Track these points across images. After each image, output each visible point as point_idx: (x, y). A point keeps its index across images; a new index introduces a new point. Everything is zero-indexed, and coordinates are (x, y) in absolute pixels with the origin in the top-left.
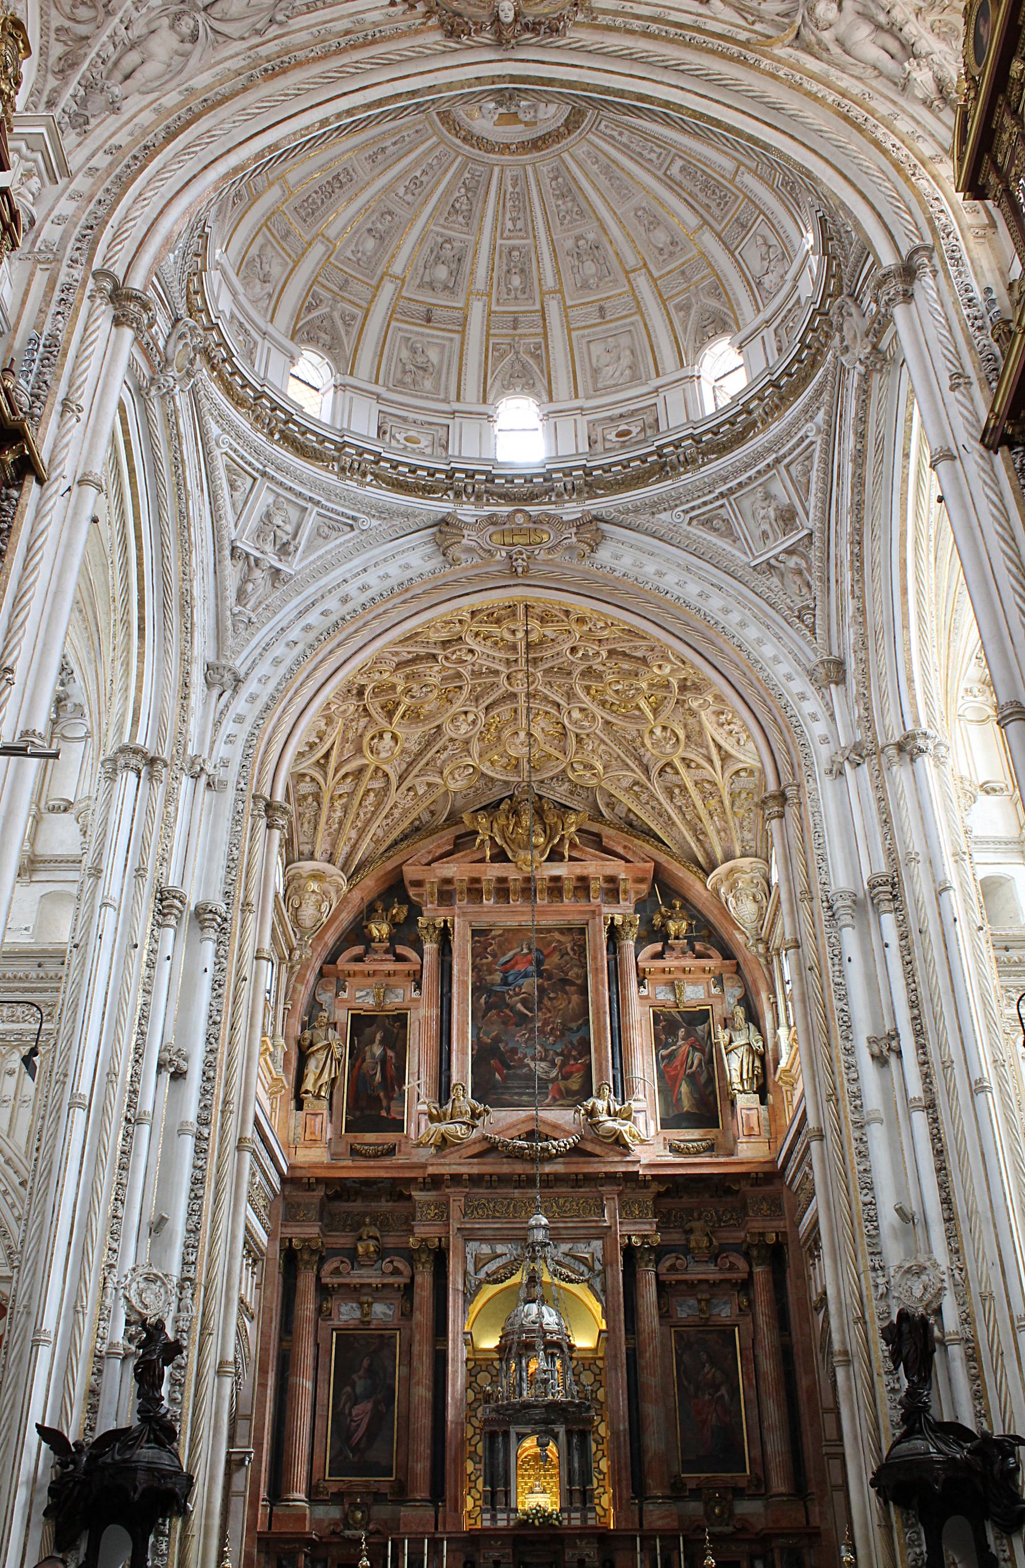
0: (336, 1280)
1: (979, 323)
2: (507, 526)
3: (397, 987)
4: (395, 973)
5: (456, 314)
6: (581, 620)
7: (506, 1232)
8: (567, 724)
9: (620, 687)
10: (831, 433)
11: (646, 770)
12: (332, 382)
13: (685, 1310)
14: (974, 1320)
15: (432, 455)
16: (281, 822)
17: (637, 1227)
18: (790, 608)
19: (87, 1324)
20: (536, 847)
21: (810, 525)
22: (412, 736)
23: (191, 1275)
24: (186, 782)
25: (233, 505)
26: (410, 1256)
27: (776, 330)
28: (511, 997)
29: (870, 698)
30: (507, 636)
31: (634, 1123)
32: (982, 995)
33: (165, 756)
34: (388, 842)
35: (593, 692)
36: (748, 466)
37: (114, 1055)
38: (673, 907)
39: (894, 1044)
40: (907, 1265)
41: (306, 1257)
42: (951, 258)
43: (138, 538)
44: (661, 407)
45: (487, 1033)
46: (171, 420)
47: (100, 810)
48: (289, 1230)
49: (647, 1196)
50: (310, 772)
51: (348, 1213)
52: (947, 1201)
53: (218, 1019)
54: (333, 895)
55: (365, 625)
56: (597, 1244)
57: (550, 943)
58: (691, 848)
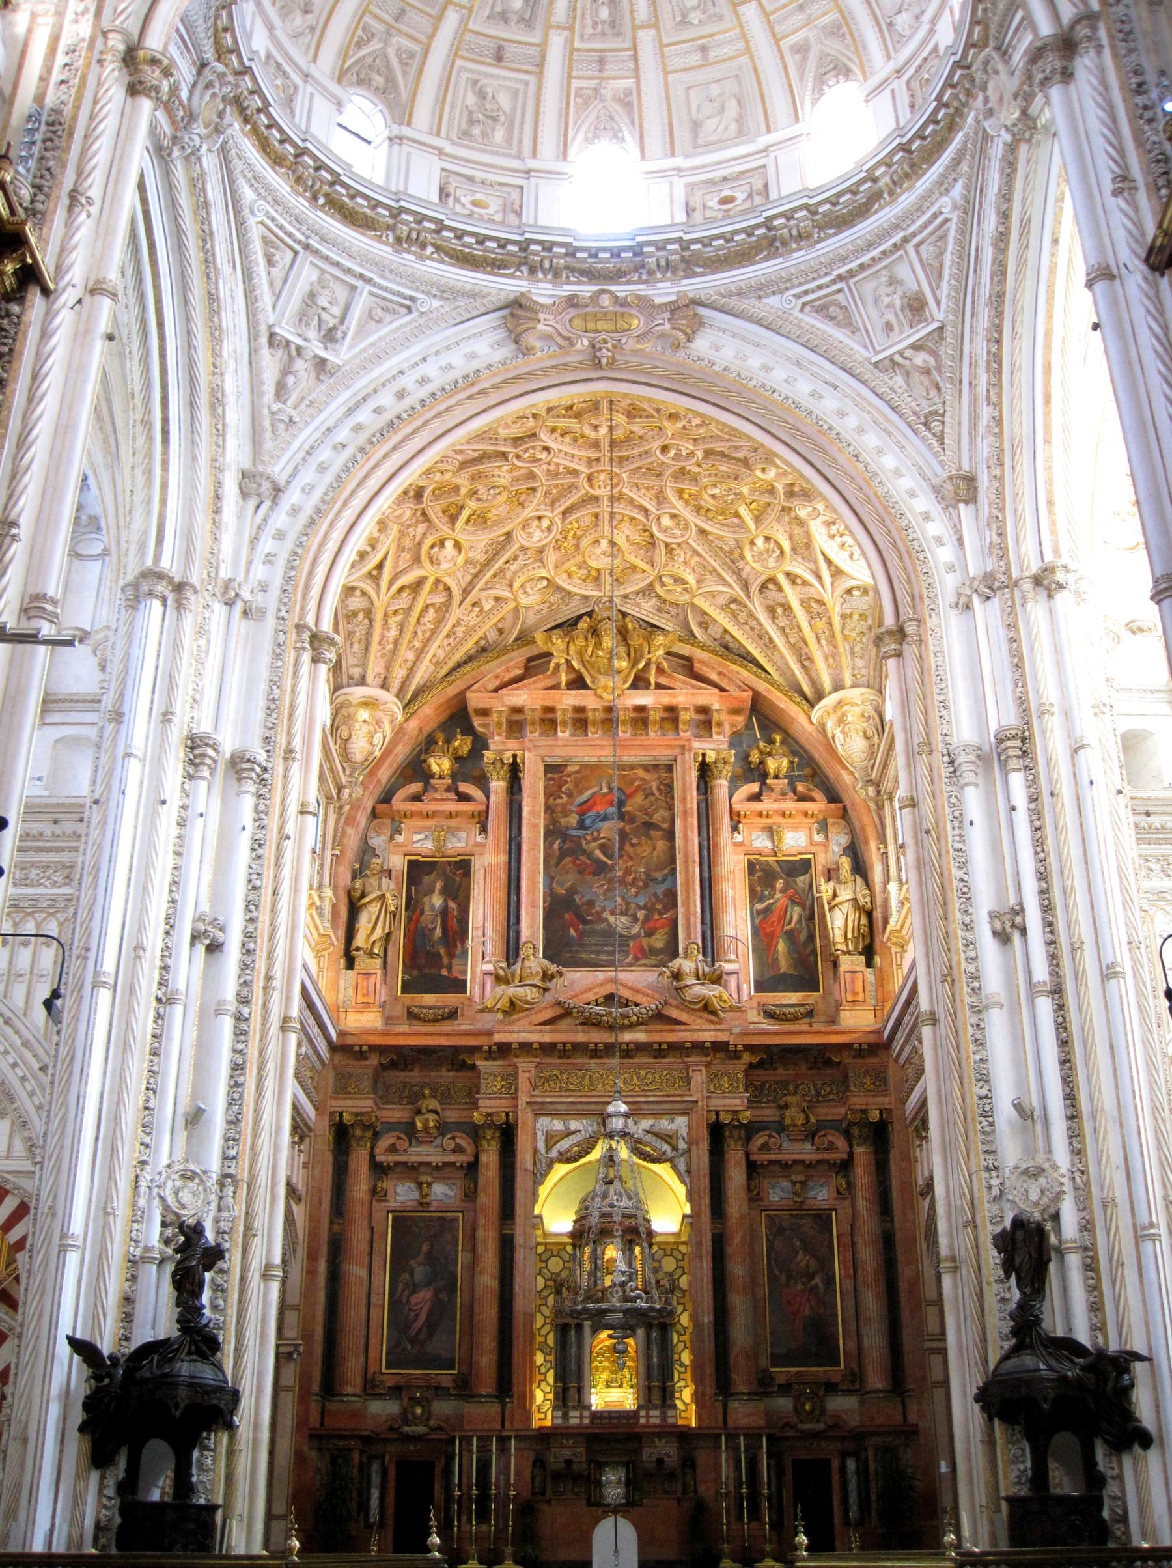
0: (391, 1159)
1: (1148, 115)
2: (590, 309)
3: (458, 829)
4: (458, 814)
5: (532, 51)
6: (673, 417)
7: (579, 1107)
8: (655, 530)
9: (717, 491)
10: (969, 210)
11: (746, 586)
12: (386, 133)
13: (778, 1193)
14: (1094, 1227)
15: (502, 223)
16: (328, 655)
18: (915, 413)
19: (119, 1227)
20: (619, 672)
21: (940, 316)
22: (478, 543)
23: (232, 1171)
24: (219, 609)
25: (271, 284)
26: (475, 1132)
27: (908, 83)
28: (588, 842)
29: (1004, 522)
30: (588, 432)
32: (1119, 868)
33: (194, 580)
34: (451, 664)
35: (686, 496)
36: (870, 245)
37: (141, 928)
38: (771, 742)
39: (1018, 920)
40: (1024, 1166)
41: (358, 1132)
42: (1121, 31)
43: (160, 325)
44: (771, 170)
45: (560, 883)
46: (197, 185)
47: (120, 645)
49: (738, 1069)
50: (361, 585)
51: (405, 1084)
52: (1070, 1097)
53: (258, 883)
54: (387, 727)
55: (425, 424)
56: (681, 1122)
57: (632, 782)
58: (793, 674)
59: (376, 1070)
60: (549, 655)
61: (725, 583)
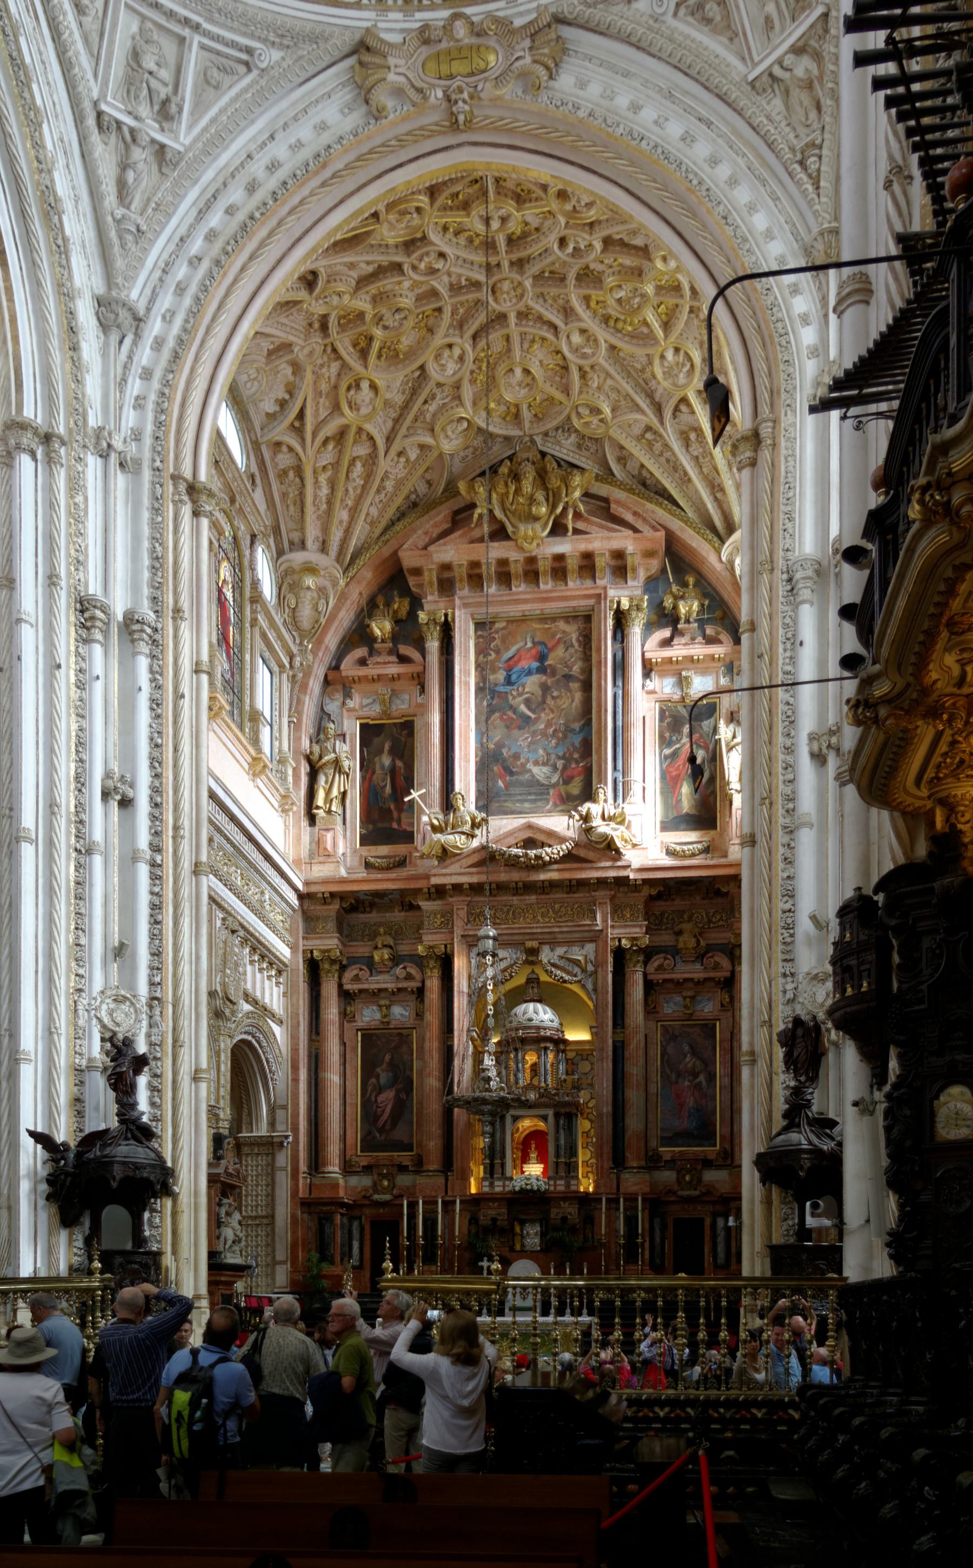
17: (628, 930)
26: (419, 961)
31: (628, 828)
41: (327, 966)
48: (310, 943)
56: (590, 948)
59: (338, 912)
60: (473, 506)
61: (642, 412)
